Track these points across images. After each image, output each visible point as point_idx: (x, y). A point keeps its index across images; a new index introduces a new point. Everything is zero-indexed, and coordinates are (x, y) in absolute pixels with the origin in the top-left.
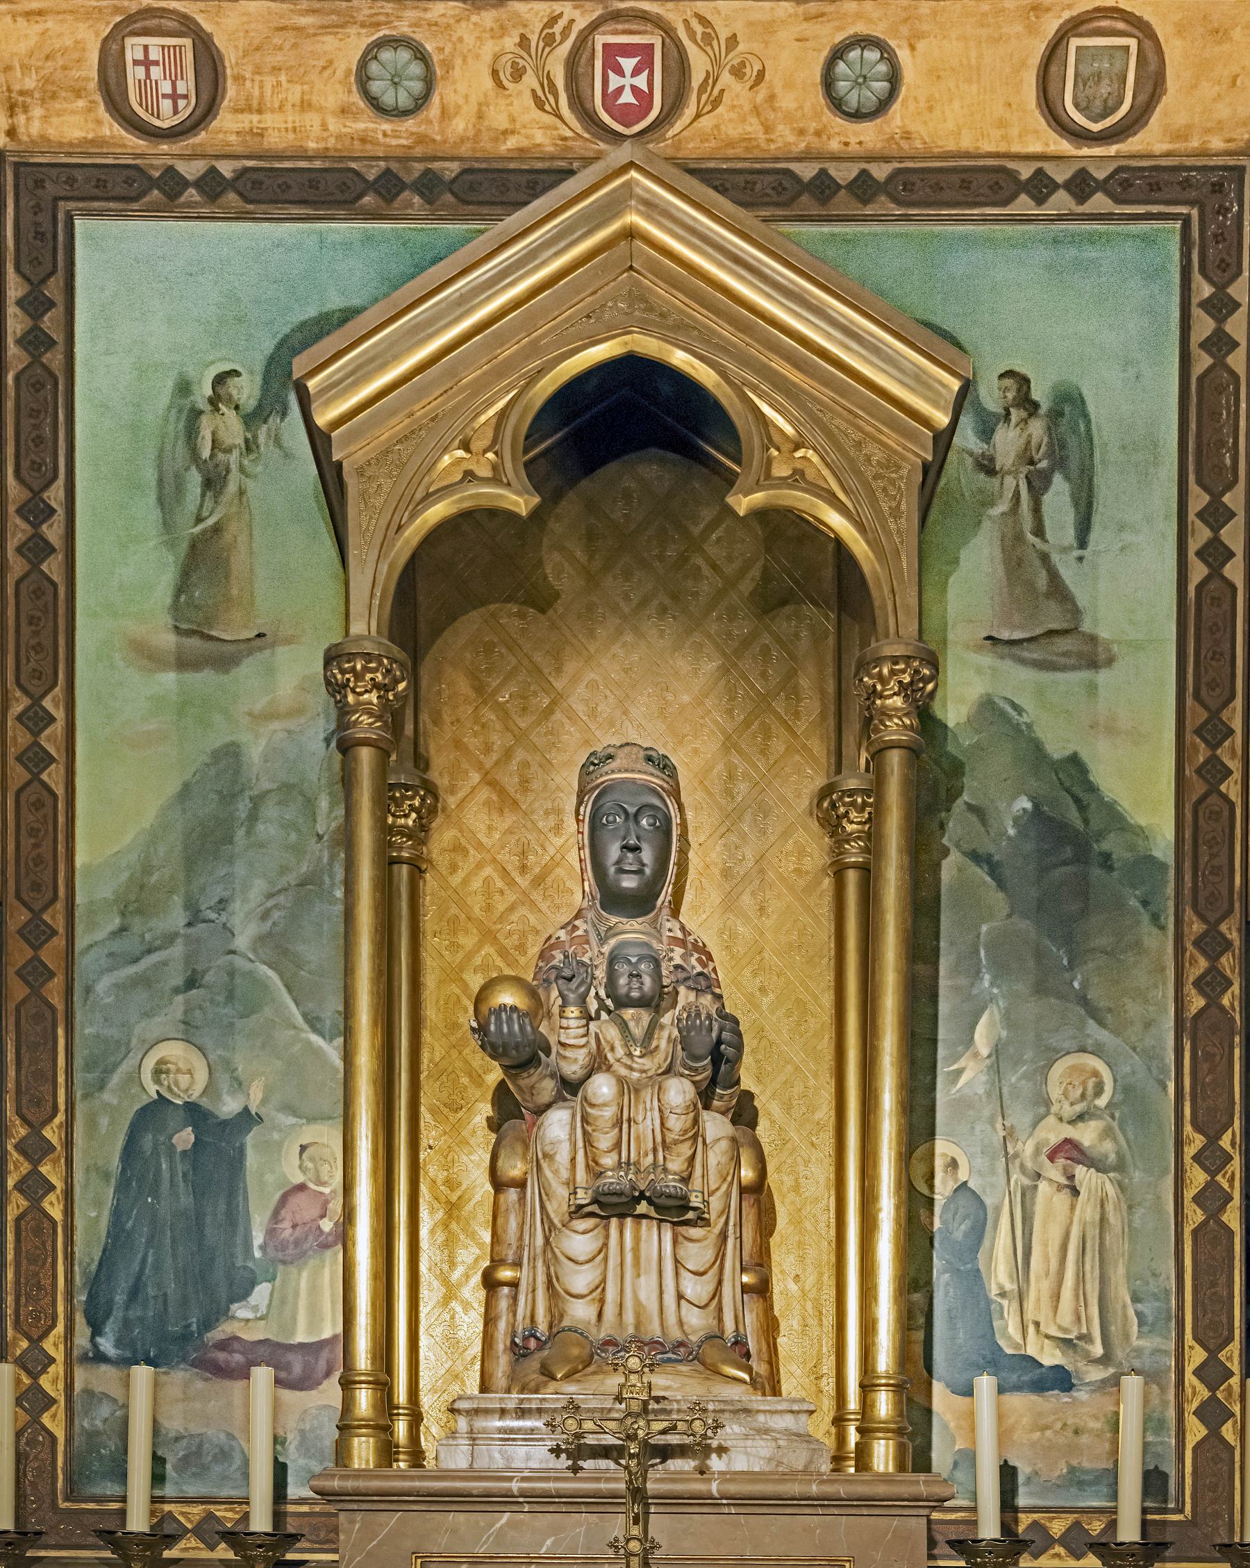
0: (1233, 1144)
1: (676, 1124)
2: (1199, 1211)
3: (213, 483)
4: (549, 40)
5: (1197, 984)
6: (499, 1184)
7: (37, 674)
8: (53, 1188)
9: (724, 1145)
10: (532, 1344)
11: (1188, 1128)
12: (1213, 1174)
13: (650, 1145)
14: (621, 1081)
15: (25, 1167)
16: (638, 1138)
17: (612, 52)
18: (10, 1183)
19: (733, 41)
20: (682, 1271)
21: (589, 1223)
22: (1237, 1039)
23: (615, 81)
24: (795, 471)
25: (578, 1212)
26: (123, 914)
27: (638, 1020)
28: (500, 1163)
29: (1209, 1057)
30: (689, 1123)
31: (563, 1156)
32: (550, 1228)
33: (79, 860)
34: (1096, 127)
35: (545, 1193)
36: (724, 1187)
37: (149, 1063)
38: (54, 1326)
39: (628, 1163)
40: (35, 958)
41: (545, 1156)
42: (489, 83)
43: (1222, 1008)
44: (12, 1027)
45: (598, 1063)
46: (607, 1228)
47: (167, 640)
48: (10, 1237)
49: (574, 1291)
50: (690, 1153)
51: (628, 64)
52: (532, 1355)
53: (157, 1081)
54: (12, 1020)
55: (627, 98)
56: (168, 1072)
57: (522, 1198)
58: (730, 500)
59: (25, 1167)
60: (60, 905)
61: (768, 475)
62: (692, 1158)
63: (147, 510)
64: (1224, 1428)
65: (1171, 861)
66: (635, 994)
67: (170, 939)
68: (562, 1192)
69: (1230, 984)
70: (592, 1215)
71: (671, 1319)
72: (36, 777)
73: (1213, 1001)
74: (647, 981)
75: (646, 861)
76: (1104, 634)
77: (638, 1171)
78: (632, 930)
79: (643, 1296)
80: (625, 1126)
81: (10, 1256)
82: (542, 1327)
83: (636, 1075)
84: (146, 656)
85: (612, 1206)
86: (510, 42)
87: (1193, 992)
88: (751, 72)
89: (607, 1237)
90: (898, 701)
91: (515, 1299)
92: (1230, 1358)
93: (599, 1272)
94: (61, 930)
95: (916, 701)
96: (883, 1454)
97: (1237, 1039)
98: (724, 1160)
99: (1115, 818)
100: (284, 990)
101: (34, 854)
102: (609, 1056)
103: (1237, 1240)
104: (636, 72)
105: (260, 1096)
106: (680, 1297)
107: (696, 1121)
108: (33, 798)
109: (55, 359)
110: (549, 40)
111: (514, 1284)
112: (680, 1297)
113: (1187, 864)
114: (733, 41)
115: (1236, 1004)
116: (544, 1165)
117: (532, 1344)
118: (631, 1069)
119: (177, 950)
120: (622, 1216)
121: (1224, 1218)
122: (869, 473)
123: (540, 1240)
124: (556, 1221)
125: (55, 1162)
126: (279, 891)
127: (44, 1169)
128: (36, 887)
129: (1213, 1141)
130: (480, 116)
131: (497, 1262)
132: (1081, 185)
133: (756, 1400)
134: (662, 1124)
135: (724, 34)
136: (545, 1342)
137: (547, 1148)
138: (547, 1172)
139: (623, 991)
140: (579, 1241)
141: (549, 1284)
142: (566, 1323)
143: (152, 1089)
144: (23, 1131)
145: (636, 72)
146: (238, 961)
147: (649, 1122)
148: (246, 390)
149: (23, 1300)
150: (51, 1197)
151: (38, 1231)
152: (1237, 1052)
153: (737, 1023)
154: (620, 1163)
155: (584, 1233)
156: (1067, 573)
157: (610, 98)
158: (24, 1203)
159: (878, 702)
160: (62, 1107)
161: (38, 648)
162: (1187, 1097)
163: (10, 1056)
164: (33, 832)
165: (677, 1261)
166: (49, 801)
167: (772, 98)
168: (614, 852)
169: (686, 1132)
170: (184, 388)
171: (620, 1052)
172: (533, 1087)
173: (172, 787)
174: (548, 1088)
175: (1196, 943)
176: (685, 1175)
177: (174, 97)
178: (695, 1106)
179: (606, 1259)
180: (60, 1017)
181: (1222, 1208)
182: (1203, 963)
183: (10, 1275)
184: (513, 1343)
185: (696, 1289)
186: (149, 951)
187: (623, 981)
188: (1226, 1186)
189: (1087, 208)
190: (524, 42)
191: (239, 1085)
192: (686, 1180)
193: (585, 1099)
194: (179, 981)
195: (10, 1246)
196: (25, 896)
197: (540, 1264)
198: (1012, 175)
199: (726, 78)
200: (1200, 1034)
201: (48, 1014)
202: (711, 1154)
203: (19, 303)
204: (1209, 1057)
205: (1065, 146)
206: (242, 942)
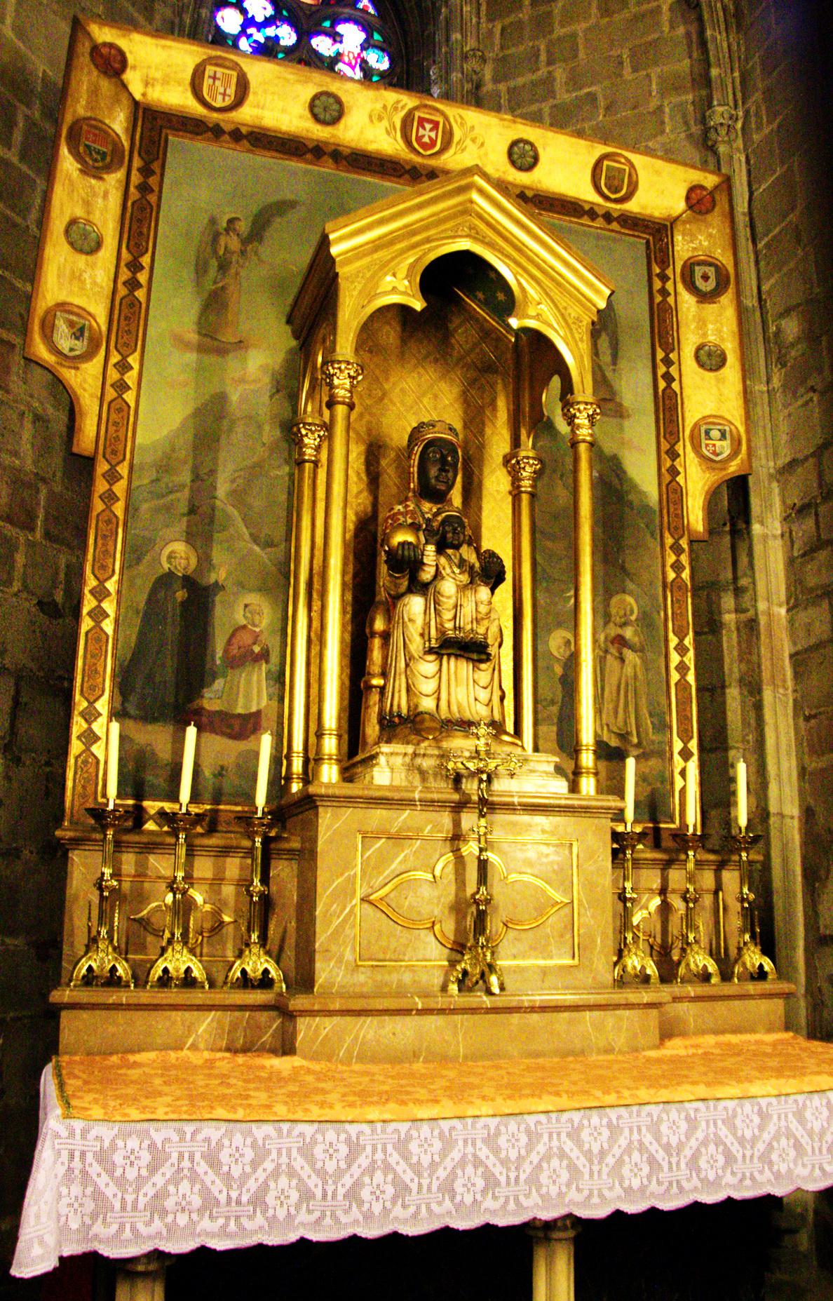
3: (223, 267)
4: (396, 109)
5: (672, 566)
7: (126, 345)
17: (422, 121)
19: (473, 128)
23: (421, 132)
33: (137, 442)
34: (613, 196)
40: (110, 489)
42: (367, 120)
44: (93, 526)
51: (428, 126)
55: (426, 140)
60: (126, 463)
63: (188, 274)
65: (657, 508)
72: (120, 396)
86: (379, 106)
88: (479, 142)
99: (634, 487)
104: (431, 130)
109: (153, 198)
110: (396, 109)
113: (665, 511)
114: (473, 128)
128: (114, 452)
130: (362, 132)
132: (608, 217)
135: (469, 124)
145: (431, 130)
148: (243, 227)
157: (419, 139)
161: (129, 332)
164: (116, 424)
166: (126, 408)
167: (486, 155)
170: (213, 221)
173: (189, 410)
177: (224, 94)
180: (121, 523)
189: (610, 227)
190: (385, 107)
198: (581, 207)
199: (468, 142)
201: (114, 520)
203: (139, 170)
204: (678, 601)
205: (599, 200)
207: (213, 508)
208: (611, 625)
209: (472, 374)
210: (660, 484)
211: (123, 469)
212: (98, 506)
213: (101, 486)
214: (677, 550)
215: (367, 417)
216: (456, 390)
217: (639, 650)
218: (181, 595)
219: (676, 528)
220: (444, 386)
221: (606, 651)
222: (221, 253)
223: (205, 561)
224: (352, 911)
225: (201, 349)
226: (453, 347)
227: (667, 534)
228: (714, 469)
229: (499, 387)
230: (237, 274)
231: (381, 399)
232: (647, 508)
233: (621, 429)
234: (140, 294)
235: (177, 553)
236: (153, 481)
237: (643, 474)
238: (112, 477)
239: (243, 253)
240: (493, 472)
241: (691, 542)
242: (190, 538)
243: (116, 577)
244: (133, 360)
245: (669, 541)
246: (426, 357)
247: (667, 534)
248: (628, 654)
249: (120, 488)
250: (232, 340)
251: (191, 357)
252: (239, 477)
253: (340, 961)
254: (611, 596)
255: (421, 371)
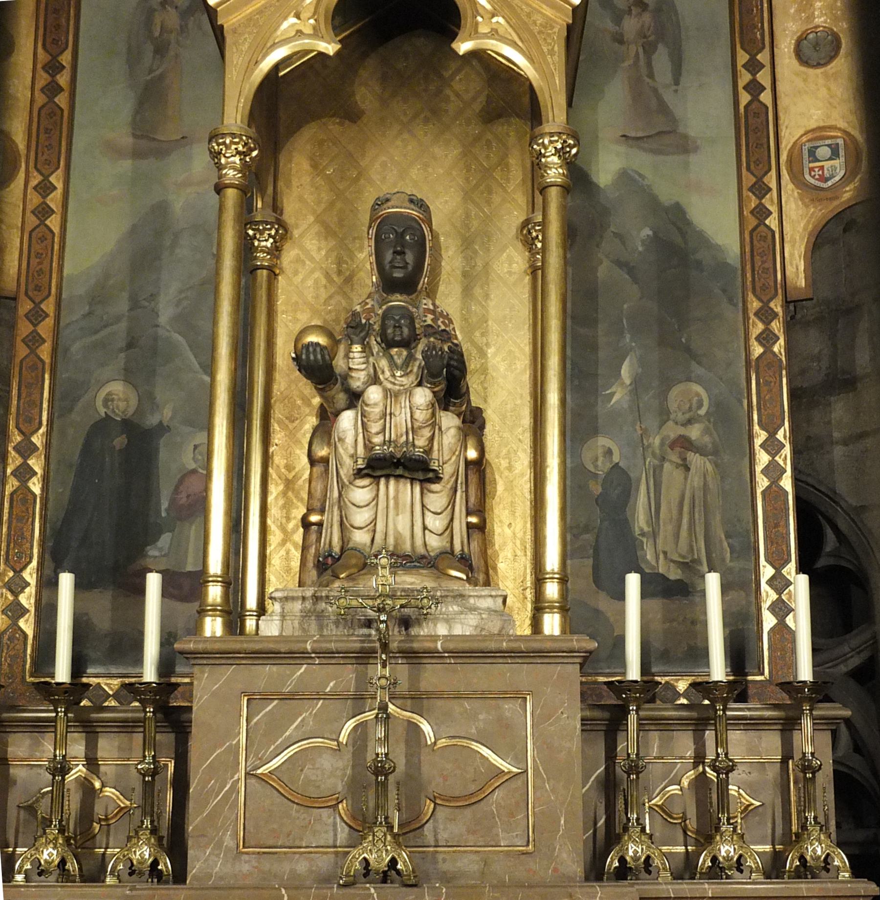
0: (785, 437)
1: (421, 416)
2: (765, 479)
6: (313, 461)
7: (48, 162)
8: (35, 473)
9: (453, 431)
10: (330, 561)
11: (756, 427)
12: (773, 456)
13: (405, 430)
14: (386, 391)
15: (19, 461)
16: (396, 426)
18: (9, 471)
20: (427, 512)
21: (366, 482)
22: (784, 372)
24: (492, 29)
25: (359, 474)
26: (90, 304)
27: (400, 355)
28: (313, 447)
29: (767, 383)
30: (428, 416)
31: (349, 439)
32: (342, 487)
33: (66, 272)
35: (339, 463)
36: (454, 458)
37: (102, 394)
38: (30, 562)
39: (390, 441)
40: (35, 331)
41: (340, 439)
43: (774, 354)
45: (375, 380)
46: (378, 484)
47: (127, 141)
48: (6, 505)
49: (357, 524)
50: (429, 435)
52: (329, 564)
53: (105, 405)
54: (17, 369)
56: (113, 400)
57: (327, 470)
58: (454, 45)
59: (19, 461)
60: (52, 299)
61: (476, 32)
62: (431, 439)
64: (787, 619)
66: (397, 338)
67: (118, 319)
68: (348, 461)
69: (778, 339)
70: (368, 475)
71: (419, 542)
72: (42, 223)
73: (768, 349)
74: (406, 331)
75: (408, 261)
76: (692, 133)
77: (396, 446)
78: (397, 301)
79: (400, 528)
80: (388, 418)
81: (5, 518)
82: (337, 549)
83: (397, 387)
84: (114, 151)
85: (380, 466)
87: (756, 343)
89: (378, 490)
90: (555, 159)
91: (320, 533)
92: (789, 573)
93: (373, 512)
94: (52, 314)
95: (566, 159)
96: (552, 624)
97: (784, 372)
98: (453, 441)
99: (703, 240)
100: (188, 348)
101: (37, 269)
102: (381, 377)
103: (790, 498)
105: (170, 414)
106: (425, 528)
107: (433, 415)
108: (40, 235)
111: (320, 524)
112: (425, 528)
113: (748, 267)
115: (783, 351)
116: (339, 445)
117: (330, 561)
118: (394, 384)
119: (123, 325)
120: (387, 477)
121: (782, 484)
122: (536, 29)
123: (336, 494)
124: (345, 480)
125: (38, 457)
126: (187, 289)
127: (31, 462)
128: (38, 288)
129: (772, 434)
131: (310, 510)
133: (468, 589)
134: (412, 416)
136: (339, 559)
137: (341, 435)
138: (341, 450)
139: (390, 337)
140: (361, 493)
141: (342, 523)
142: (351, 545)
143: (102, 411)
144: (19, 439)
146: (160, 331)
147: (403, 415)
149: (12, 545)
150: (34, 479)
151: (24, 501)
152: (784, 380)
153: (462, 355)
154: (384, 441)
155: (363, 487)
156: (668, 97)
158: (16, 483)
159: (543, 160)
160: (45, 422)
161: (49, 147)
162: (755, 408)
163: (15, 392)
164: (38, 255)
165: (423, 506)
166: (49, 236)
168: (389, 256)
169: (427, 421)
171: (388, 374)
172: (333, 397)
174: (342, 398)
175: (756, 314)
176: (426, 448)
178: (433, 405)
179: (377, 504)
180: (47, 368)
181: (780, 477)
182: (760, 327)
183: (5, 530)
184: (319, 561)
185: (436, 523)
186: (105, 326)
187: (390, 331)
188: (781, 463)
191: (155, 407)
192: (428, 451)
193: (363, 401)
194: (122, 344)
195: (6, 511)
196: (30, 293)
197: (336, 509)
200: (761, 369)
202: (445, 437)
204: (767, 383)
206: (163, 320)
207: (156, 338)
208: (670, 423)
209: (475, 129)
210: (742, 233)
211: (49, 306)
212: (22, 351)
213: (24, 328)
214: (765, 315)
215: (339, 205)
216: (455, 152)
217: (712, 453)
218: (120, 441)
219: (764, 288)
220: (437, 151)
221: (663, 459)
222: (157, 34)
223: (147, 400)
224: (234, 789)
225: (137, 154)
226: (447, 100)
227: (751, 296)
228: (820, 200)
229: (512, 140)
230: (177, 56)
231: (357, 179)
232: (722, 269)
233: (686, 166)
234: (62, 100)
235: (115, 395)
236: (84, 316)
237: (718, 222)
238: (36, 316)
239: (183, 29)
240: (503, 249)
241: (787, 302)
242: (129, 375)
243: (43, 430)
244: (56, 179)
245: (755, 304)
246: (416, 116)
247: (751, 296)
248: (695, 459)
249: (45, 328)
250: (175, 137)
251: (127, 164)
252: (186, 298)
253: (219, 845)
254: (669, 388)
255: (406, 136)
